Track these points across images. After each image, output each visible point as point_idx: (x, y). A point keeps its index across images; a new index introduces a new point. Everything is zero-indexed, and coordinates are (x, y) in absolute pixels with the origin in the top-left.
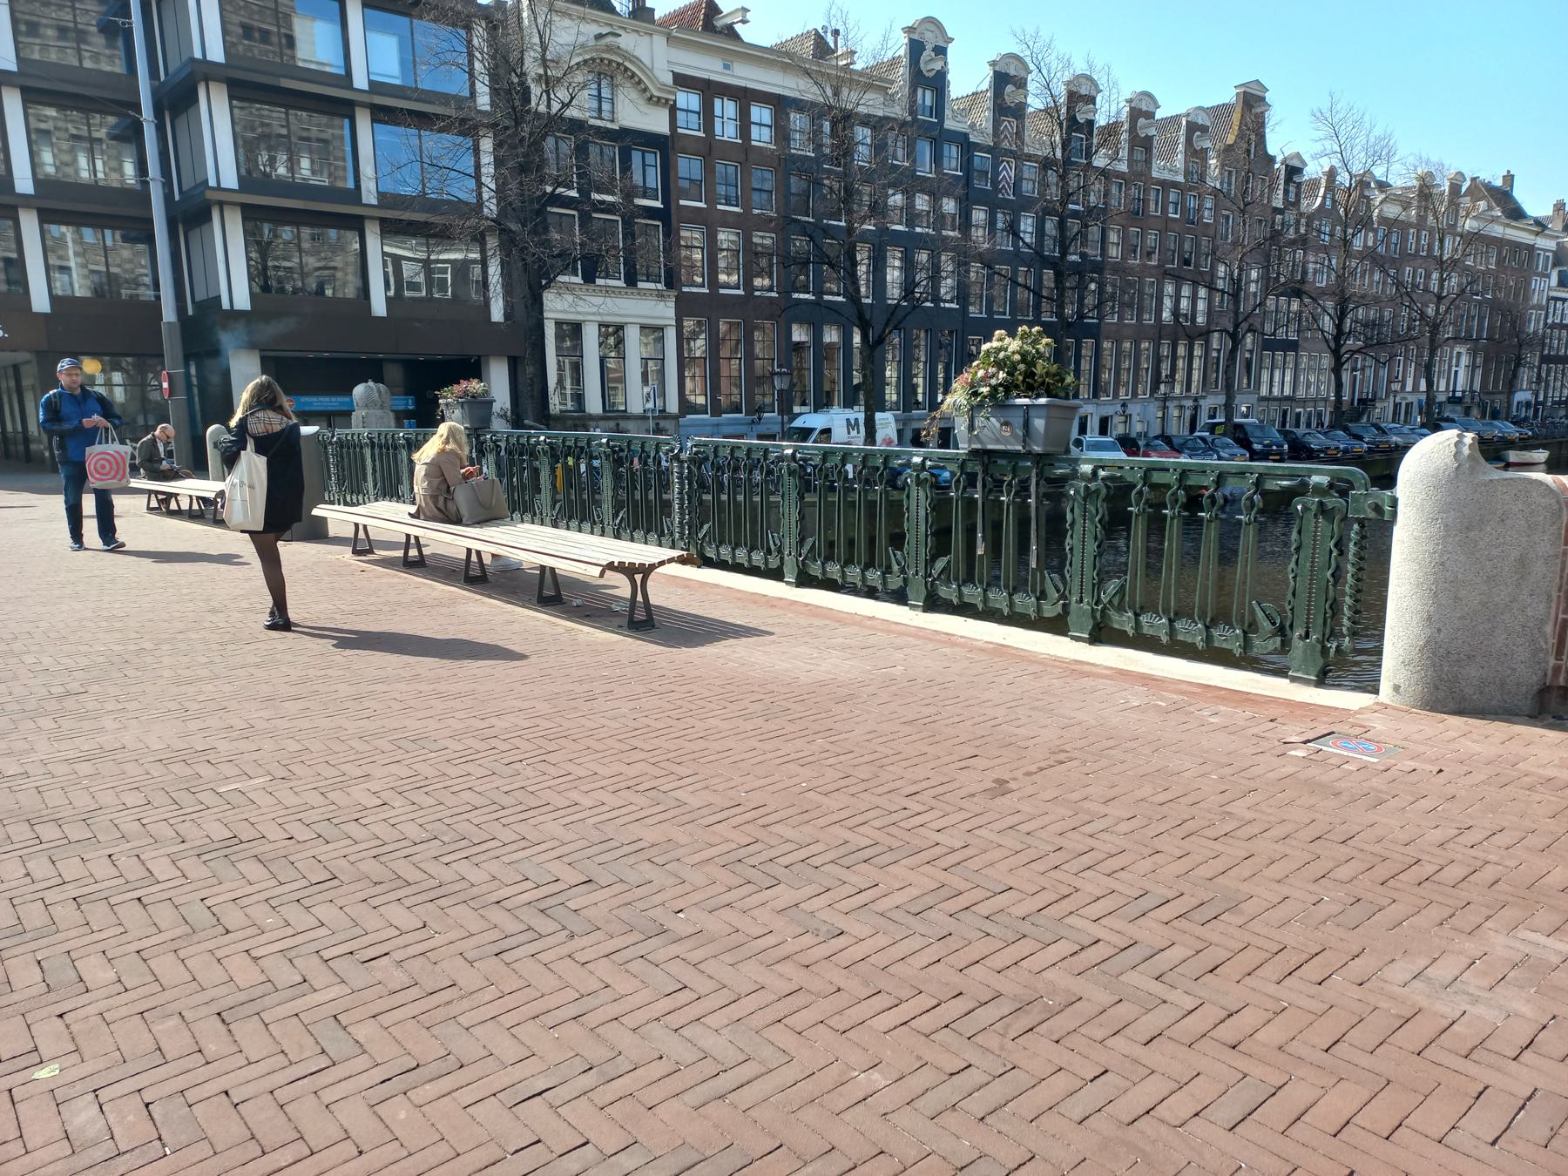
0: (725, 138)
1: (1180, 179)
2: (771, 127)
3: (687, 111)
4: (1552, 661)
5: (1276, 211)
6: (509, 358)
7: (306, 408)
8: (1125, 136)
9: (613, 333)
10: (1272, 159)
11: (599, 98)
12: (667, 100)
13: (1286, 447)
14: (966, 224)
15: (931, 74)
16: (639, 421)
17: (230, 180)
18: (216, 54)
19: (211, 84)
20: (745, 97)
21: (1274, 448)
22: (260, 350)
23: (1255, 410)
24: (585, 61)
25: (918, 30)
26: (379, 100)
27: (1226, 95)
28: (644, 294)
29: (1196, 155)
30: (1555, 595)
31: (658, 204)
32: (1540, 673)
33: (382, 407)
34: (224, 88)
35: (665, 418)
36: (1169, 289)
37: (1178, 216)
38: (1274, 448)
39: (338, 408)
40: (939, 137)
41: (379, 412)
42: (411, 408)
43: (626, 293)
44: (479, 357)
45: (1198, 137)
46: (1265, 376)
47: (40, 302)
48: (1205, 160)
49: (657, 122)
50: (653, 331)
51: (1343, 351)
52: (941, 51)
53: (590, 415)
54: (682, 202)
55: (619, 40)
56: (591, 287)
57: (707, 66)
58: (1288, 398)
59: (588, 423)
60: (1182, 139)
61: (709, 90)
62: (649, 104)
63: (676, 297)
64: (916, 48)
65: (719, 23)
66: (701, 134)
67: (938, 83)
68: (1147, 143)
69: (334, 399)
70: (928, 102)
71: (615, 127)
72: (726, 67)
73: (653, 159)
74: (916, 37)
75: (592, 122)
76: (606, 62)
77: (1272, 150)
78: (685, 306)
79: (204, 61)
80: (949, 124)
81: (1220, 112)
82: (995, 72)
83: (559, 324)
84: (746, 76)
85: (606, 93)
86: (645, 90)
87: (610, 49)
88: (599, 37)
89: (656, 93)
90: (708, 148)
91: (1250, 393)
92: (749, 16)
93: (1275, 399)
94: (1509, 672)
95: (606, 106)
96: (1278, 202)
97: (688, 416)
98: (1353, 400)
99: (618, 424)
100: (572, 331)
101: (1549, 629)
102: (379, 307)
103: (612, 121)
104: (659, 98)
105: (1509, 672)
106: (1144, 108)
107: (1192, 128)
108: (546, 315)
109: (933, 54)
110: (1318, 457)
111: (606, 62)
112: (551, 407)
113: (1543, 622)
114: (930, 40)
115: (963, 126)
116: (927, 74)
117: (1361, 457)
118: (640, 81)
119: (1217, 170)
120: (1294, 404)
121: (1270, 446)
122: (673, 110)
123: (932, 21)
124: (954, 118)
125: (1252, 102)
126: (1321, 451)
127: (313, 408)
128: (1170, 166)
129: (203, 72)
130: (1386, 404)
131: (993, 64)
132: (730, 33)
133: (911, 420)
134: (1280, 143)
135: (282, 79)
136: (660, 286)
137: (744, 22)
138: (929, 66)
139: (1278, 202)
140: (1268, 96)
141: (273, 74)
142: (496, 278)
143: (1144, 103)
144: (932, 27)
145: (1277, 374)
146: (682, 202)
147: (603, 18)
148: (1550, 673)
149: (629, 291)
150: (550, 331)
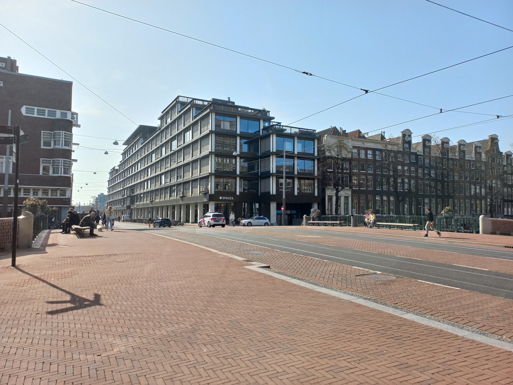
1: (474, 159)
2: (372, 154)
5: (504, 166)
8: (457, 150)
10: (502, 153)
15: (407, 141)
17: (275, 172)
20: (366, 149)
22: (277, 202)
26: (300, 156)
29: (478, 154)
36: (473, 187)
37: (474, 168)
42: (295, 213)
45: (478, 149)
46: (505, 209)
47: (238, 193)
48: (481, 156)
49: (349, 156)
52: (410, 136)
61: (359, 148)
64: (404, 136)
66: (357, 157)
67: (410, 142)
68: (464, 152)
72: (363, 144)
77: (501, 151)
78: (353, 192)
80: (412, 151)
82: (423, 139)
83: (328, 196)
90: (359, 160)
91: (501, 214)
107: (476, 147)
109: (408, 136)
114: (407, 133)
123: (408, 130)
125: (494, 140)
128: (471, 156)
131: (422, 137)
132: (364, 137)
138: (407, 139)
140: (498, 137)
150: (327, 197)
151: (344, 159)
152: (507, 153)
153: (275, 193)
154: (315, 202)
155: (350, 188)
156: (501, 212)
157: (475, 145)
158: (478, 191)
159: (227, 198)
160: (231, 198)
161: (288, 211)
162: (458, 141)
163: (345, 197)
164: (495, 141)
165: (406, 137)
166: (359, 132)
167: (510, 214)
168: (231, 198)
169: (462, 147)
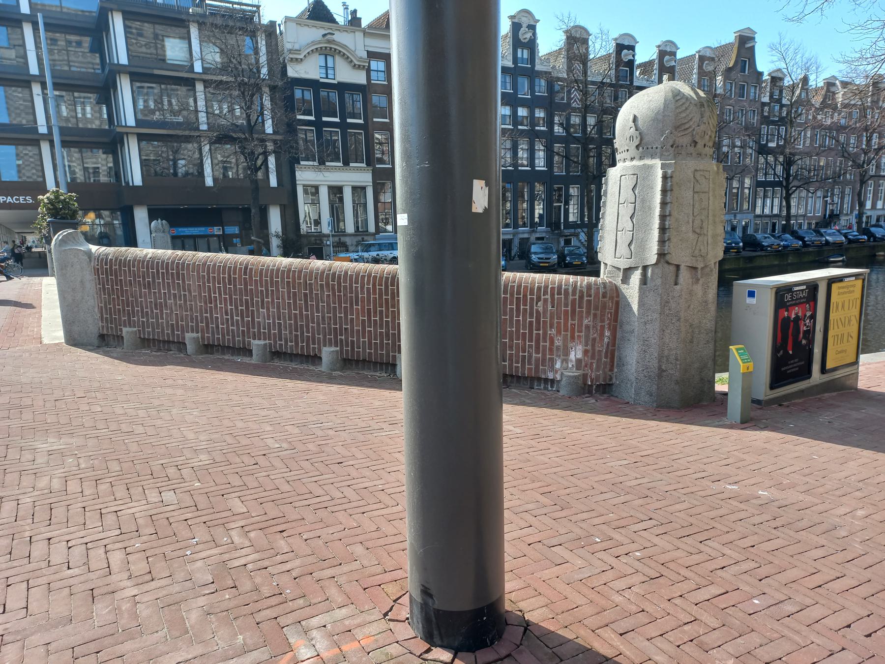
3: (377, 71)
4: (100, 324)
5: (764, 104)
6: (281, 205)
7: (182, 234)
8: (656, 66)
9: (336, 191)
10: (761, 74)
11: (326, 67)
12: (364, 66)
13: (741, 244)
14: (550, 124)
15: (526, 41)
16: (352, 237)
18: (124, 60)
19: (121, 75)
21: (733, 245)
22: (148, 206)
23: (752, 223)
24: (317, 49)
25: (517, 18)
27: (729, 38)
28: (329, 169)
30: (96, 296)
31: (361, 121)
32: (98, 329)
33: (164, 232)
34: (128, 76)
35: (367, 235)
38: (733, 245)
39: (198, 234)
40: (532, 74)
41: (162, 235)
42: (237, 232)
43: (343, 169)
44: (266, 205)
45: (707, 64)
46: (759, 202)
49: (360, 78)
50: (359, 190)
51: (791, 186)
52: (532, 28)
53: (324, 234)
54: (375, 120)
55: (334, 36)
56: (322, 167)
58: (776, 216)
59: (323, 238)
60: (696, 66)
63: (372, 170)
66: (386, 83)
69: (196, 229)
70: (525, 56)
71: (335, 82)
73: (359, 97)
74: (516, 21)
75: (322, 80)
76: (333, 50)
77: (760, 68)
79: (118, 64)
80: (538, 67)
81: (723, 50)
85: (330, 64)
86: (351, 61)
87: (329, 42)
88: (324, 35)
89: (357, 63)
91: (748, 213)
93: (767, 216)
94: (87, 328)
95: (330, 72)
96: (766, 99)
97: (381, 234)
98: (825, 215)
99: (340, 239)
100: (314, 190)
101: (96, 310)
102: (209, 182)
103: (334, 79)
104: (359, 66)
105: (87, 328)
106: (669, 50)
107: (702, 59)
108: (297, 183)
109: (527, 29)
110: (767, 250)
112: (302, 230)
113: (94, 307)
114: (525, 21)
115: (549, 68)
116: (523, 41)
117: (797, 250)
118: (348, 57)
119: (722, 83)
120: (780, 219)
121: (731, 244)
122: (368, 71)
124: (542, 64)
126: (768, 246)
127: (185, 234)
129: (120, 69)
130: (851, 217)
131: (566, 32)
133: (518, 233)
134: (765, 64)
135: (155, 70)
136: (316, 163)
139: (766, 99)
140: (756, 36)
141: (149, 68)
142: (207, 165)
143: (668, 47)
144: (527, 15)
145: (768, 201)
146: (375, 120)
147: (334, 26)
148: (101, 328)
149: (344, 168)
150: (300, 190)
151: (342, 88)
152: (773, 75)
153: (138, 180)
154: (274, 204)
155: (368, 164)
156: (737, 210)
157: (700, 54)
159: (9, 199)
160: (25, 200)
161: (215, 228)
162: (658, 43)
164: (748, 45)
165: (522, 29)
167: (768, 213)
168: (25, 200)
169: (667, 58)
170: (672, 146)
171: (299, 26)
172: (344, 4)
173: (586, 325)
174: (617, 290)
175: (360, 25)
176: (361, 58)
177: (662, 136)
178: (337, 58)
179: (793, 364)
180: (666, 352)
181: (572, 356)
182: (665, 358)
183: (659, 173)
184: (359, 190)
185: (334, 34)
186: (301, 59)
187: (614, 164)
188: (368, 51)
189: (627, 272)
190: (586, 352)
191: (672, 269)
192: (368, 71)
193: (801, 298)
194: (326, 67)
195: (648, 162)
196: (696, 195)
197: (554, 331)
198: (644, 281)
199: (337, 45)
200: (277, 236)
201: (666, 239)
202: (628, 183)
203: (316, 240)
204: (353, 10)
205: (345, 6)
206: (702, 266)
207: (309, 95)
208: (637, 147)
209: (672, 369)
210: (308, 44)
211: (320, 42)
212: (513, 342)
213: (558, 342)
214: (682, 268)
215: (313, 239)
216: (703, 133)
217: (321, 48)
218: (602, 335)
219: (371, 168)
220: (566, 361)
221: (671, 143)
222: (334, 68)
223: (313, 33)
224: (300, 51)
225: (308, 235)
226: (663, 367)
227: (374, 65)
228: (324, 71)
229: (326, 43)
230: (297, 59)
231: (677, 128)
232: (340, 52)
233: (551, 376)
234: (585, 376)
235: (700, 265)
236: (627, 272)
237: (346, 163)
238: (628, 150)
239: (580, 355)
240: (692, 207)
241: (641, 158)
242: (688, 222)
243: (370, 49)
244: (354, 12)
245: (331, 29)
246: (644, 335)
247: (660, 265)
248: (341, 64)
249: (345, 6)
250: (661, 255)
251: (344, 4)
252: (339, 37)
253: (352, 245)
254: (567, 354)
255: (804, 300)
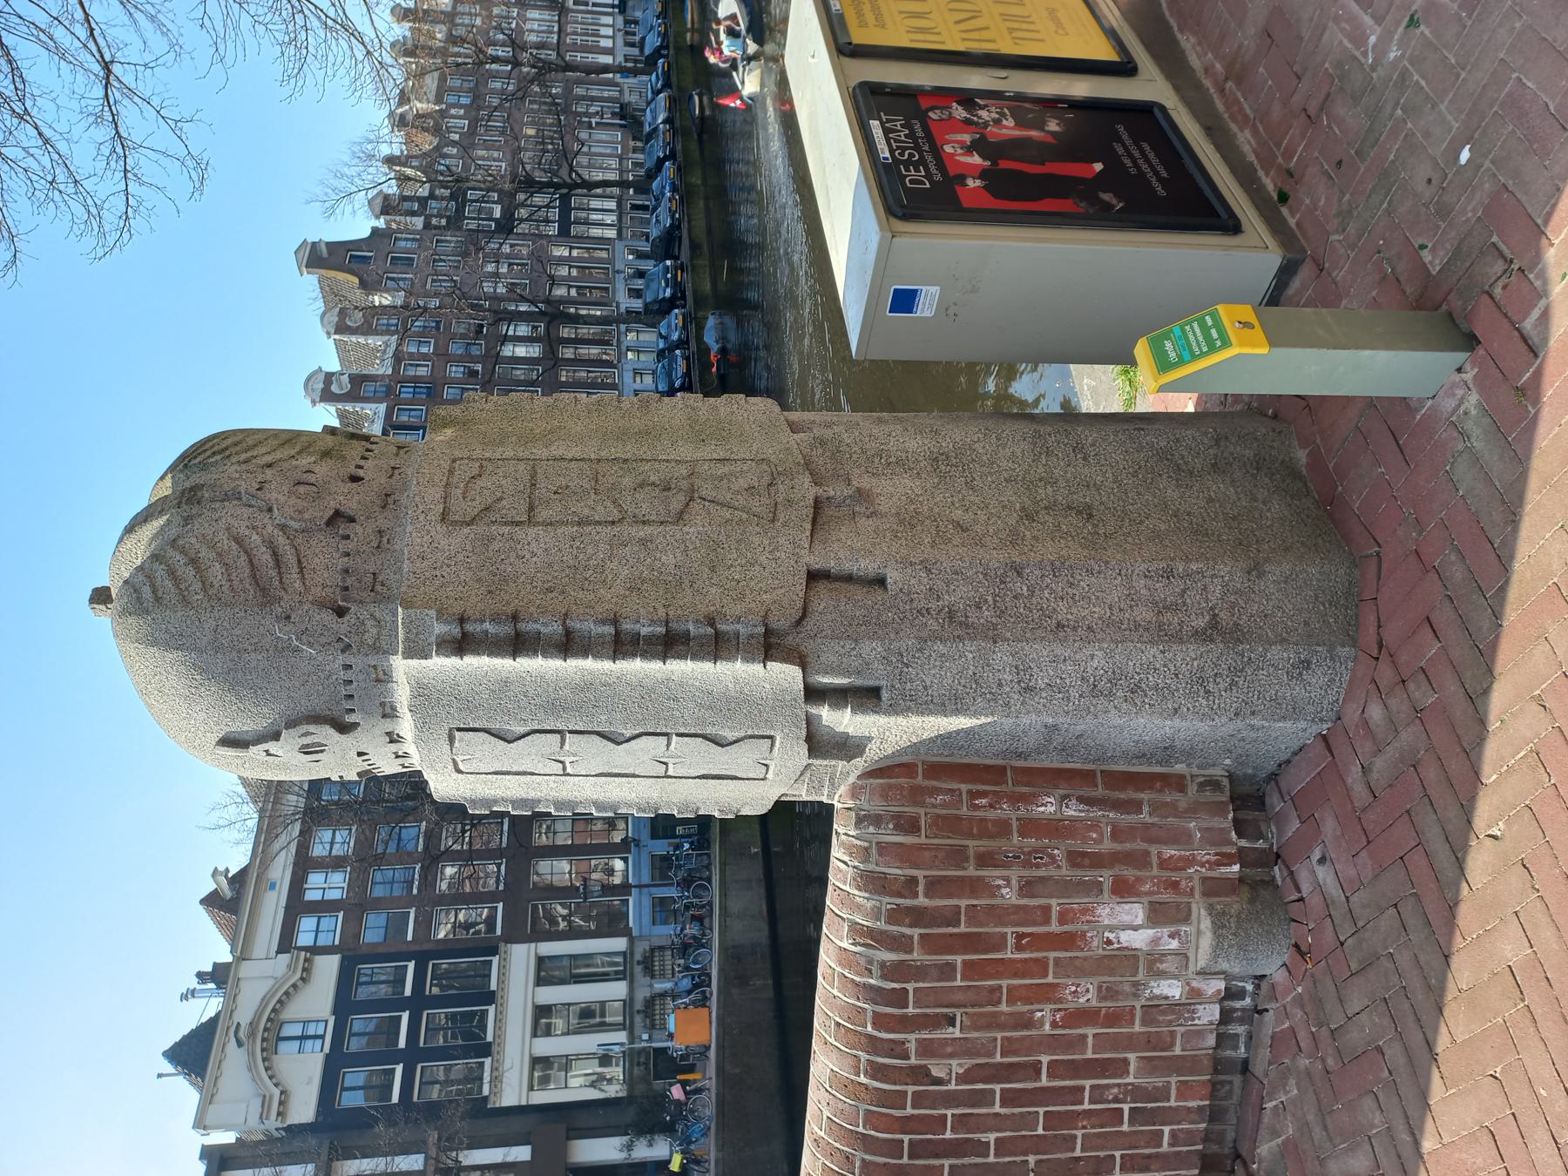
0: (345, 885)
3: (317, 932)
5: (427, 225)
6: (569, 1138)
8: (349, 407)
9: (542, 1015)
10: (375, 231)
11: (303, 1038)
12: (306, 960)
13: (668, 263)
16: (636, 985)
20: (304, 864)
21: (669, 276)
23: (630, 243)
24: (264, 1060)
27: (310, 283)
29: (371, 322)
31: (411, 966)
35: (632, 954)
36: (508, 351)
37: (433, 341)
38: (669, 276)
43: (501, 1005)
44: (567, 1169)
46: (596, 232)
49: (328, 968)
50: (546, 972)
51: (568, 180)
54: (410, 938)
56: (495, 1049)
57: (273, 906)
58: (619, 205)
60: (354, 339)
61: (297, 906)
62: (309, 980)
63: (507, 942)
65: (227, 892)
68: (358, 380)
72: (273, 886)
75: (327, 1049)
77: (366, 233)
81: (331, 293)
84: (281, 870)
85: (296, 1030)
86: (294, 986)
87: (252, 1034)
88: (240, 1044)
90: (355, 907)
91: (613, 251)
92: (221, 868)
93: (620, 219)
95: (311, 1032)
96: (418, 222)
97: (631, 924)
98: (621, 126)
99: (638, 1012)
100: (541, 1064)
103: (326, 1021)
104: (304, 970)
106: (321, 386)
107: (341, 328)
110: (679, 219)
111: (265, 1054)
112: (620, 1095)
117: (679, 169)
119: (386, 295)
120: (625, 197)
121: (667, 281)
122: (315, 950)
125: (320, 257)
126: (673, 217)
128: (379, 361)
130: (626, 86)
132: (239, 880)
134: (357, 224)
137: (227, 870)
139: (418, 222)
140: (310, 240)
143: (316, 386)
145: (594, 217)
146: (410, 938)
149: (499, 1001)
150: (540, 1098)
151: (344, 1005)
152: (378, 209)
155: (494, 951)
156: (608, 268)
157: (333, 331)
158: (523, 330)
162: (308, 402)
163: (535, 1035)
164: (325, 254)
166: (212, 901)
167: (615, 218)
169: (334, 388)
170: (341, 612)
171: (216, 1098)
172: (184, 997)
173: (1021, 895)
174: (878, 772)
175: (227, 966)
176: (289, 966)
177: (297, 650)
178: (286, 1015)
179: (1134, 160)
180: (1144, 614)
181: (1138, 940)
182: (1167, 617)
183: (442, 665)
184: (546, 972)
185: (239, 1023)
186: (282, 1093)
187: (414, 784)
188: (278, 952)
189: (819, 744)
190: (1123, 890)
191: (823, 599)
192: (315, 950)
193: (911, 135)
194: (303, 1038)
195: (402, 694)
196: (543, 514)
197: (1044, 1014)
198: (866, 697)
199: (263, 1012)
200: (629, 1147)
201: (710, 630)
202: (481, 752)
203: (638, 1064)
204: (197, 980)
205: (190, 994)
206: (807, 480)
207: (355, 1076)
208: (344, 728)
209: (1205, 588)
210: (254, 1080)
211: (252, 1054)
212: (1078, 1159)
213: (1086, 994)
214: (817, 561)
215: (636, 1071)
216: (302, 489)
217: (263, 1050)
218: (1055, 828)
219: (502, 946)
220: (1153, 962)
221: (328, 617)
222: (306, 1022)
223: (233, 1063)
224: (264, 1097)
225: (629, 1081)
226: (1201, 622)
227: (304, 939)
228: (309, 1043)
229: (254, 1042)
230: (281, 1103)
231: (266, 596)
232: (274, 1010)
233: (1209, 1014)
234: (1213, 888)
235: (806, 490)
236: (819, 744)
237: (490, 998)
238: (360, 754)
239: (1135, 912)
240: (588, 529)
241: (389, 713)
242: (644, 542)
243: (275, 947)
244: (201, 976)
245: (228, 1028)
246: (1074, 693)
247: (808, 646)
248: (294, 1010)
249: (190, 994)
250: (770, 647)
251: (184, 997)
252: (244, 1016)
253: (651, 986)
254: (1129, 958)
255: (917, 127)
